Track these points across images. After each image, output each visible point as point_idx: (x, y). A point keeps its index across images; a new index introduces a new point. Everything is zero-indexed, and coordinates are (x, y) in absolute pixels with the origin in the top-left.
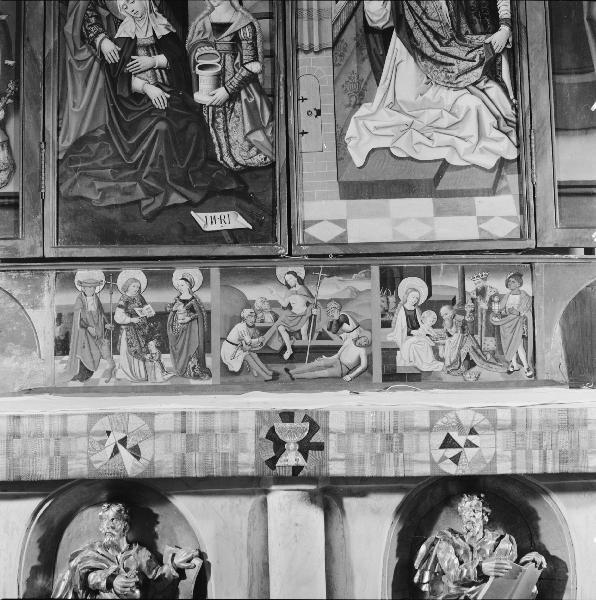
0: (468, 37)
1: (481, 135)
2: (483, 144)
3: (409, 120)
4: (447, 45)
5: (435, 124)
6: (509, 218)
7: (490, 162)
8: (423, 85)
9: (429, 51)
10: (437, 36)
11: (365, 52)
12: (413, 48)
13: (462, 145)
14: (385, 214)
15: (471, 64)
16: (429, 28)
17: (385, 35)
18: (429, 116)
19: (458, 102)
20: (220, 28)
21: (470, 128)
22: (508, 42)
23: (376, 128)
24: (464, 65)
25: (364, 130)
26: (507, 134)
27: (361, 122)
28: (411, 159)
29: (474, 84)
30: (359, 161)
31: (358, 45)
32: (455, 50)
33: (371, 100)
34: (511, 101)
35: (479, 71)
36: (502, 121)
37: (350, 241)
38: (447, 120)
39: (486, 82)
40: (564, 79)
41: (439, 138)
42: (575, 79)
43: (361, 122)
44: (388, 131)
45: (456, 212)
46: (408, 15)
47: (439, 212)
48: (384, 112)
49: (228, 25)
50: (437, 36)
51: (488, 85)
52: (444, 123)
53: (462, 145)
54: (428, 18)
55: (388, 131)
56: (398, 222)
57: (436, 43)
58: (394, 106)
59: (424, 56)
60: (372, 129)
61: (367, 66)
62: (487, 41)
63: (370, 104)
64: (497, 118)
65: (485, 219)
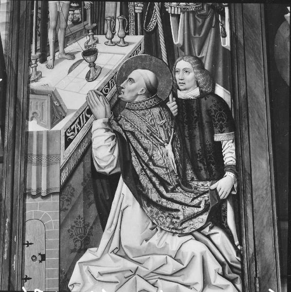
1: (206, 282)
3: (133, 266)
4: (173, 191)
5: (160, 271)
8: (148, 230)
9: (154, 197)
10: (163, 182)
11: (92, 197)
12: (140, 194)
15: (196, 210)
16: (156, 175)
17: (111, 181)
18: (153, 262)
21: (195, 275)
22: (233, 189)
23: (101, 274)
24: (189, 211)
25: (88, 277)
26: (233, 281)
27: (85, 268)
29: (199, 230)
31: (85, 190)
32: (179, 196)
33: (96, 245)
34: (235, 247)
35: (205, 217)
36: (227, 268)
38: (172, 266)
39: (211, 228)
43: (85, 268)
44: (113, 278)
46: (135, 161)
48: (108, 257)
50: (163, 182)
51: (213, 231)
54: (154, 165)
55: (113, 278)
57: (162, 189)
58: (120, 251)
59: (150, 202)
60: (96, 275)
61: (93, 212)
62: (213, 187)
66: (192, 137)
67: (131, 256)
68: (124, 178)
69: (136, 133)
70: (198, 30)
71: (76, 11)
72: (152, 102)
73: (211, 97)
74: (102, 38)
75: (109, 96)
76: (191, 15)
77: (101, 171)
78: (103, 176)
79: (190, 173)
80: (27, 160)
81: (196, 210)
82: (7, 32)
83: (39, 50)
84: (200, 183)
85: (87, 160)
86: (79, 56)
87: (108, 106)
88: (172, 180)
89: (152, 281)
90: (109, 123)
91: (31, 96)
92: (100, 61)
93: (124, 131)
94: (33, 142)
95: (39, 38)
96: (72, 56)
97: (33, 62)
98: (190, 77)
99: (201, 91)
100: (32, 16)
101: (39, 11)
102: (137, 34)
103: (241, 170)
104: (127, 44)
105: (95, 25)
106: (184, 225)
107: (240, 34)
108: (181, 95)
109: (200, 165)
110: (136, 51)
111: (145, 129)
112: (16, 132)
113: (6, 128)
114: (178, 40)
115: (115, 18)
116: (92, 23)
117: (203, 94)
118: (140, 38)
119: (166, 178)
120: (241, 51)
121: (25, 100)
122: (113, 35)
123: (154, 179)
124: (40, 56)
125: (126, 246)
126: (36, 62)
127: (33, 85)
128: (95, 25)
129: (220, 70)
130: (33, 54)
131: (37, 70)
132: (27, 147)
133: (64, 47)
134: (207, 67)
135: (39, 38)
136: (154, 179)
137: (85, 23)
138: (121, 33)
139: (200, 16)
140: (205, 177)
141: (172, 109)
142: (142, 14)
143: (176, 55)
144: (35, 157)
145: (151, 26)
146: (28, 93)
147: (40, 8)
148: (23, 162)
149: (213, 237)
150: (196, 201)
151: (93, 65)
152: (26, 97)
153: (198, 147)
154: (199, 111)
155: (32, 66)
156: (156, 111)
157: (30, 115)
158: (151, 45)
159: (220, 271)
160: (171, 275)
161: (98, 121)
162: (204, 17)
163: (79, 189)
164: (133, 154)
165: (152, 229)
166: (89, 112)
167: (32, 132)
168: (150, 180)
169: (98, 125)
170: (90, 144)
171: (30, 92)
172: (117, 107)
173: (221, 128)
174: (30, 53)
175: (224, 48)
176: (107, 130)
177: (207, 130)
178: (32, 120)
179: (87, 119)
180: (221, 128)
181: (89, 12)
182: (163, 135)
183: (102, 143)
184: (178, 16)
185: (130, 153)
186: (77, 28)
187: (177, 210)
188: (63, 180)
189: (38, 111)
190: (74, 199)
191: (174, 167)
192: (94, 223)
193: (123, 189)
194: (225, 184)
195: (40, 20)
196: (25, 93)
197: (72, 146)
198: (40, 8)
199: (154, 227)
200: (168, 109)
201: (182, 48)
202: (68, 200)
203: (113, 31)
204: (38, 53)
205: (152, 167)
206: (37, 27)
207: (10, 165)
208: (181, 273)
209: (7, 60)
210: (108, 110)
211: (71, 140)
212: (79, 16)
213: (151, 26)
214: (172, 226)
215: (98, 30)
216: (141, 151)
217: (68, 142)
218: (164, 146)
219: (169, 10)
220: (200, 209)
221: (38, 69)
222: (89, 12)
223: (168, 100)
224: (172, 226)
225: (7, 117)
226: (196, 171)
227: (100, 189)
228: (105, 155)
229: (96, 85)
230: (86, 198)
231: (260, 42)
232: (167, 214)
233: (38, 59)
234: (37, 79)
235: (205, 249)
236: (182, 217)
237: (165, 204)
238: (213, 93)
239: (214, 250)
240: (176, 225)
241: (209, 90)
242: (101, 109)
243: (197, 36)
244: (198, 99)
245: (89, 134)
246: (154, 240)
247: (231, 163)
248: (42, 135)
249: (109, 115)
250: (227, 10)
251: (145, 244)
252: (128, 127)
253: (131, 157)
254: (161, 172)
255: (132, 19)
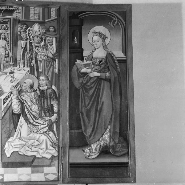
0: (44, 117)
2: (47, 151)
3: (24, 143)
4: (37, 120)
5: (33, 145)
6: (54, 174)
7: (49, 156)
8: (29, 132)
9: (32, 121)
10: (34, 117)
11: (12, 121)
12: (27, 120)
13: (41, 151)
14: (16, 172)
15: (45, 126)
16: (32, 114)
17: (19, 116)
18: (31, 142)
19: (40, 138)
21: (44, 146)
22: (56, 119)
23: (14, 145)
24: (42, 126)
25: (10, 146)
26: (55, 148)
27: (9, 143)
28: (24, 155)
29: (45, 132)
30: (8, 156)
31: (10, 118)
32: (39, 121)
33: (13, 136)
34: (56, 138)
35: (47, 128)
36: (53, 144)
37: (4, 181)
38: (37, 143)
39: (49, 132)
40: (73, 131)
41: (34, 149)
42: (76, 131)
43: (9, 143)
44: (18, 146)
45: (38, 172)
46: (26, 110)
47: (33, 172)
48: (17, 140)
50: (34, 117)
51: (49, 132)
52: (35, 144)
53: (41, 151)
54: (32, 111)
55: (18, 146)
56: (20, 175)
57: (34, 119)
58: (20, 138)
59: (30, 123)
60: (13, 145)
61: (12, 126)
62: (50, 119)
63: (12, 137)
64: (52, 143)
65: (47, 174)
66: (44, 103)
67: (24, 140)
68: (22, 115)
69: (26, 100)
70: (47, 66)
71: (7, 58)
72: (32, 90)
73: (51, 89)
74: (15, 68)
75: (18, 88)
76: (45, 61)
77: (15, 113)
78: (15, 114)
79: (43, 114)
81: (45, 126)
84: (46, 117)
85: (10, 109)
86: (8, 74)
87: (17, 91)
88: (37, 116)
89: (31, 148)
90: (18, 97)
92: (16, 75)
93: (23, 100)
96: (6, 73)
98: (44, 82)
99: (48, 87)
102: (27, 67)
103: (59, 113)
104: (25, 70)
105: (13, 63)
106: (41, 131)
107: (61, 68)
108: (41, 88)
109: (46, 111)
110: (27, 73)
111: (29, 99)
114: (40, 70)
115: (20, 61)
116: (13, 62)
117: (48, 88)
118: (28, 69)
119: (36, 115)
120: (61, 74)
122: (20, 67)
123: (32, 116)
125: (22, 137)
128: (13, 63)
129: (54, 80)
133: (3, 70)
134: (50, 79)
136: (32, 116)
137: (10, 62)
138: (22, 66)
139: (48, 61)
140: (48, 115)
141: (38, 93)
142: (29, 60)
143: (40, 75)
145: (32, 64)
149: (50, 135)
150: (45, 123)
151: (13, 77)
153: (46, 106)
154: (47, 94)
156: (33, 93)
158: (32, 72)
159: (51, 145)
160: (36, 146)
161: (14, 96)
162: (49, 62)
163: (8, 118)
164: (25, 107)
165: (31, 132)
166: (11, 93)
168: (30, 116)
169: (14, 97)
170: (12, 104)
172: (20, 92)
173: (53, 100)
175: (56, 73)
176: (17, 99)
177: (49, 100)
179: (11, 95)
180: (53, 100)
181: (11, 58)
182: (35, 102)
183: (15, 103)
184: (41, 61)
185: (24, 107)
186: (7, 64)
187: (38, 126)
188: (3, 115)
190: (6, 121)
191: (38, 112)
192: (12, 129)
193: (22, 119)
194: (54, 118)
197: (6, 104)
199: (31, 131)
200: (37, 93)
201: (42, 72)
202: (4, 122)
203: (19, 65)
205: (31, 112)
208: (39, 145)
210: (18, 93)
211: (5, 102)
212: (8, 60)
213: (32, 64)
214: (37, 131)
215: (15, 65)
216: (28, 107)
217: (4, 103)
218: (35, 105)
219: (38, 59)
220: (46, 126)
222: (11, 58)
223: (37, 90)
224: (37, 131)
226: (45, 113)
227: (15, 118)
228: (16, 108)
229: (15, 84)
230: (10, 121)
231: (67, 72)
232: (35, 127)
235: (47, 138)
236: (40, 128)
237: (35, 124)
238: (51, 88)
239: (49, 138)
240: (38, 131)
241: (50, 87)
242: (15, 92)
243: (47, 68)
244: (47, 90)
245: (11, 100)
246: (31, 135)
247: (56, 111)
249: (18, 94)
250: (57, 60)
251: (28, 136)
252: (24, 98)
253: (24, 109)
254: (34, 113)
255: (26, 62)
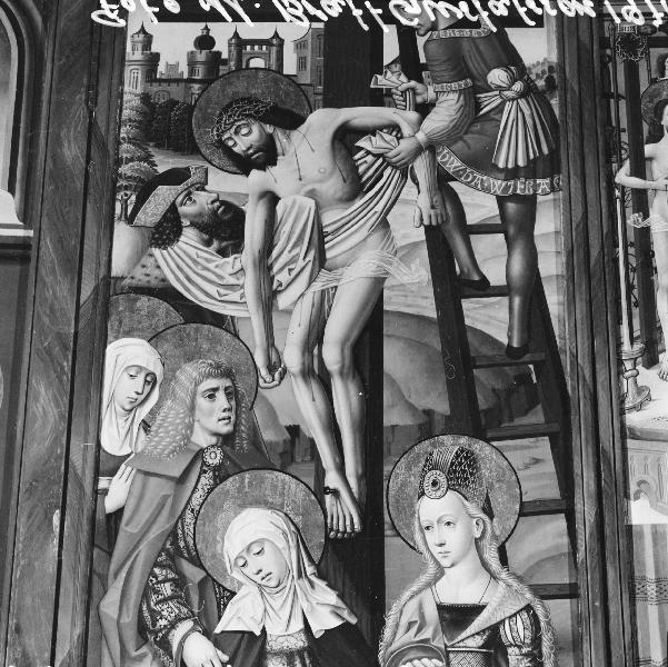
20: (456, 616)
49: (476, 610)
80: (634, 591)
82: (561, 297)
83: (638, 337)
91: (630, 443)
94: (643, 549)
95: (636, 311)
97: (628, 365)
100: (616, 260)
101: (631, 250)
112: (606, 526)
113: (578, 516)
121: (618, 451)
124: (643, 352)
126: (635, 365)
127: (633, 419)
130: (626, 347)
131: (640, 384)
132: (631, 563)
135: (636, 311)
144: (654, 586)
146: (623, 437)
147: (632, 245)
148: (626, 597)
152: (618, 445)
155: (626, 374)
157: (633, 488)
167: (641, 526)
171: (625, 433)
174: (619, 344)
178: (637, 498)
189: (651, 477)
195: (634, 270)
196: (617, 435)
198: (632, 245)
204: (638, 346)
206: (630, 288)
207: (597, 604)
209: (566, 361)
221: (641, 381)
225: (578, 492)
233: (639, 360)
234: (641, 403)
248: (642, 532)
